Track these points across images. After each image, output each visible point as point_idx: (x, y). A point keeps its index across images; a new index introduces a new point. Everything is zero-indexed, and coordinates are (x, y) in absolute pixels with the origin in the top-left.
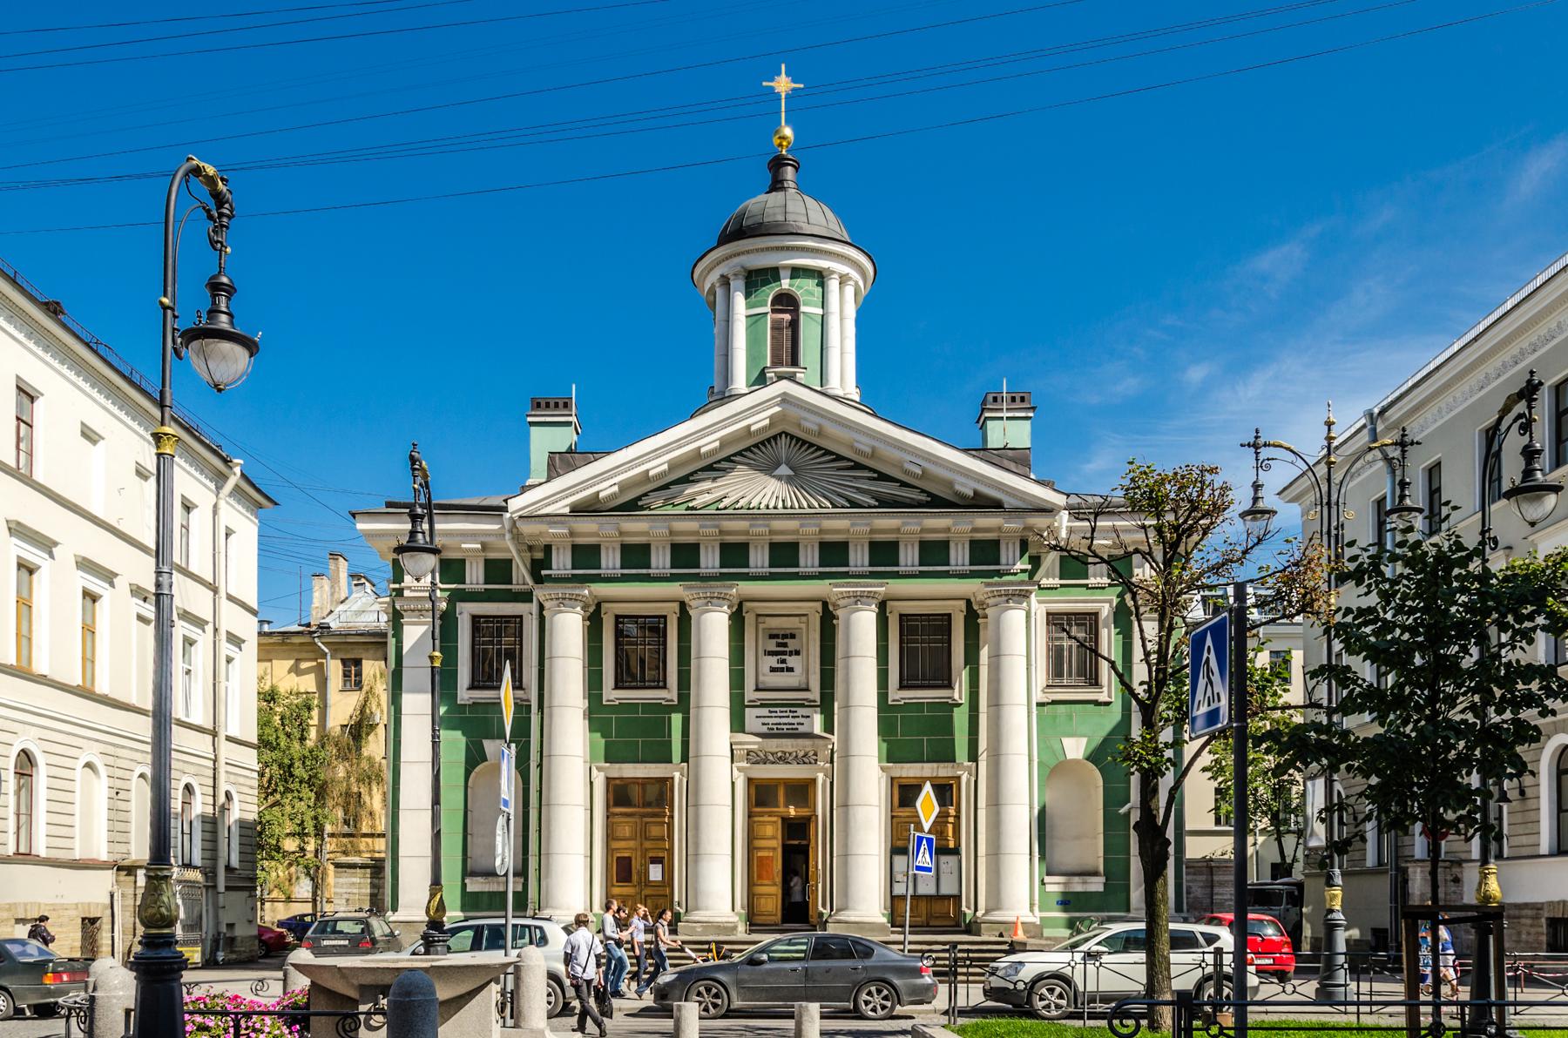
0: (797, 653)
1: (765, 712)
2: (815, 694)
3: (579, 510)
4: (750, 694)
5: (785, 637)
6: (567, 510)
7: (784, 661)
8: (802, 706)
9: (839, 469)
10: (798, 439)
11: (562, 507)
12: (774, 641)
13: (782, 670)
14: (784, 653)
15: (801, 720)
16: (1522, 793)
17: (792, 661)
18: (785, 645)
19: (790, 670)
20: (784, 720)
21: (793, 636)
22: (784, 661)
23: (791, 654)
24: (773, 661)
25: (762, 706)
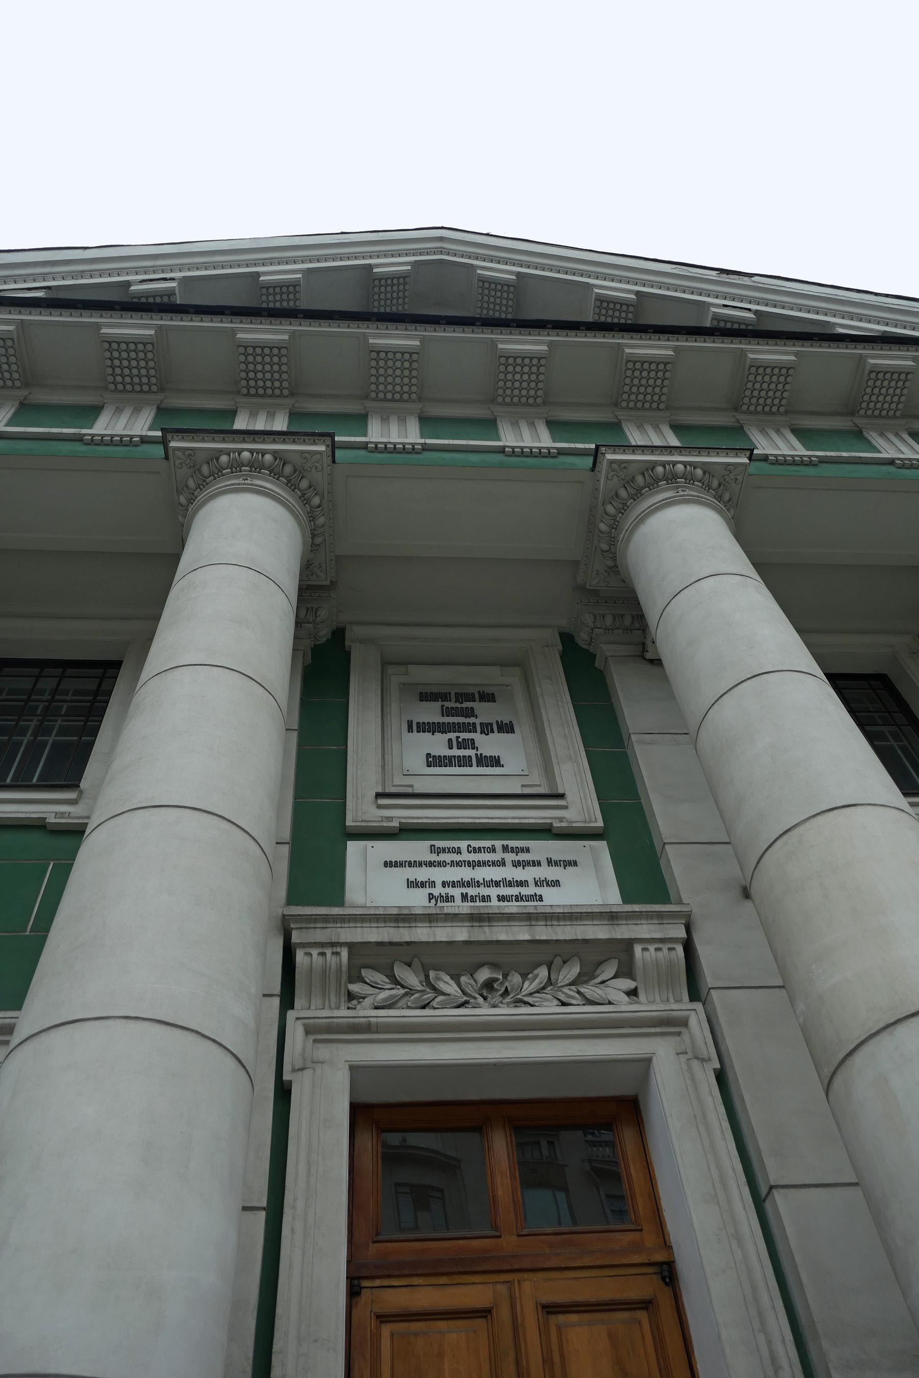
0: (506, 728)
1: (418, 849)
2: (582, 804)
7: (471, 744)
8: (545, 832)
12: (437, 705)
13: (465, 762)
15: (551, 873)
17: (488, 744)
19: (495, 762)
21: (487, 697)
23: (487, 729)
24: (438, 744)
25: (407, 832)
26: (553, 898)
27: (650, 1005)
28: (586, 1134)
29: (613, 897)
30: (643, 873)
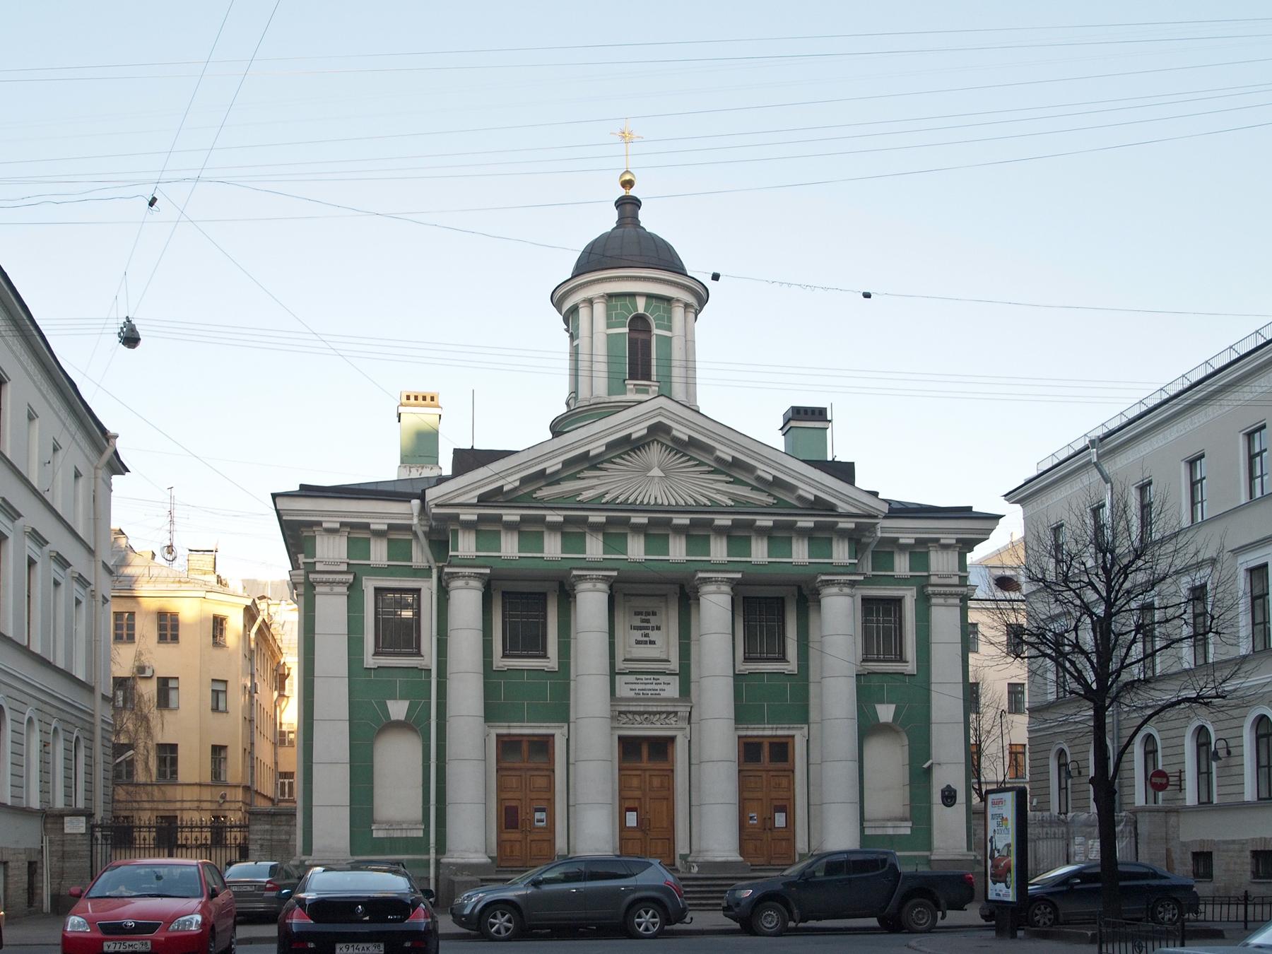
0: (658, 628)
1: (632, 678)
2: (674, 665)
3: (484, 500)
4: (620, 665)
5: (648, 614)
6: (475, 501)
7: (647, 635)
9: (702, 473)
10: (667, 447)
11: (472, 497)
13: (646, 643)
14: (647, 628)
16: (1229, 753)
17: (654, 635)
18: (648, 621)
19: (652, 642)
20: (646, 685)
21: (654, 614)
22: (647, 635)
24: (638, 635)
25: (631, 673)
26: (663, 695)
27: (680, 725)
28: (662, 747)
29: (677, 696)
30: (685, 691)
